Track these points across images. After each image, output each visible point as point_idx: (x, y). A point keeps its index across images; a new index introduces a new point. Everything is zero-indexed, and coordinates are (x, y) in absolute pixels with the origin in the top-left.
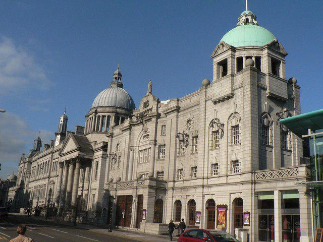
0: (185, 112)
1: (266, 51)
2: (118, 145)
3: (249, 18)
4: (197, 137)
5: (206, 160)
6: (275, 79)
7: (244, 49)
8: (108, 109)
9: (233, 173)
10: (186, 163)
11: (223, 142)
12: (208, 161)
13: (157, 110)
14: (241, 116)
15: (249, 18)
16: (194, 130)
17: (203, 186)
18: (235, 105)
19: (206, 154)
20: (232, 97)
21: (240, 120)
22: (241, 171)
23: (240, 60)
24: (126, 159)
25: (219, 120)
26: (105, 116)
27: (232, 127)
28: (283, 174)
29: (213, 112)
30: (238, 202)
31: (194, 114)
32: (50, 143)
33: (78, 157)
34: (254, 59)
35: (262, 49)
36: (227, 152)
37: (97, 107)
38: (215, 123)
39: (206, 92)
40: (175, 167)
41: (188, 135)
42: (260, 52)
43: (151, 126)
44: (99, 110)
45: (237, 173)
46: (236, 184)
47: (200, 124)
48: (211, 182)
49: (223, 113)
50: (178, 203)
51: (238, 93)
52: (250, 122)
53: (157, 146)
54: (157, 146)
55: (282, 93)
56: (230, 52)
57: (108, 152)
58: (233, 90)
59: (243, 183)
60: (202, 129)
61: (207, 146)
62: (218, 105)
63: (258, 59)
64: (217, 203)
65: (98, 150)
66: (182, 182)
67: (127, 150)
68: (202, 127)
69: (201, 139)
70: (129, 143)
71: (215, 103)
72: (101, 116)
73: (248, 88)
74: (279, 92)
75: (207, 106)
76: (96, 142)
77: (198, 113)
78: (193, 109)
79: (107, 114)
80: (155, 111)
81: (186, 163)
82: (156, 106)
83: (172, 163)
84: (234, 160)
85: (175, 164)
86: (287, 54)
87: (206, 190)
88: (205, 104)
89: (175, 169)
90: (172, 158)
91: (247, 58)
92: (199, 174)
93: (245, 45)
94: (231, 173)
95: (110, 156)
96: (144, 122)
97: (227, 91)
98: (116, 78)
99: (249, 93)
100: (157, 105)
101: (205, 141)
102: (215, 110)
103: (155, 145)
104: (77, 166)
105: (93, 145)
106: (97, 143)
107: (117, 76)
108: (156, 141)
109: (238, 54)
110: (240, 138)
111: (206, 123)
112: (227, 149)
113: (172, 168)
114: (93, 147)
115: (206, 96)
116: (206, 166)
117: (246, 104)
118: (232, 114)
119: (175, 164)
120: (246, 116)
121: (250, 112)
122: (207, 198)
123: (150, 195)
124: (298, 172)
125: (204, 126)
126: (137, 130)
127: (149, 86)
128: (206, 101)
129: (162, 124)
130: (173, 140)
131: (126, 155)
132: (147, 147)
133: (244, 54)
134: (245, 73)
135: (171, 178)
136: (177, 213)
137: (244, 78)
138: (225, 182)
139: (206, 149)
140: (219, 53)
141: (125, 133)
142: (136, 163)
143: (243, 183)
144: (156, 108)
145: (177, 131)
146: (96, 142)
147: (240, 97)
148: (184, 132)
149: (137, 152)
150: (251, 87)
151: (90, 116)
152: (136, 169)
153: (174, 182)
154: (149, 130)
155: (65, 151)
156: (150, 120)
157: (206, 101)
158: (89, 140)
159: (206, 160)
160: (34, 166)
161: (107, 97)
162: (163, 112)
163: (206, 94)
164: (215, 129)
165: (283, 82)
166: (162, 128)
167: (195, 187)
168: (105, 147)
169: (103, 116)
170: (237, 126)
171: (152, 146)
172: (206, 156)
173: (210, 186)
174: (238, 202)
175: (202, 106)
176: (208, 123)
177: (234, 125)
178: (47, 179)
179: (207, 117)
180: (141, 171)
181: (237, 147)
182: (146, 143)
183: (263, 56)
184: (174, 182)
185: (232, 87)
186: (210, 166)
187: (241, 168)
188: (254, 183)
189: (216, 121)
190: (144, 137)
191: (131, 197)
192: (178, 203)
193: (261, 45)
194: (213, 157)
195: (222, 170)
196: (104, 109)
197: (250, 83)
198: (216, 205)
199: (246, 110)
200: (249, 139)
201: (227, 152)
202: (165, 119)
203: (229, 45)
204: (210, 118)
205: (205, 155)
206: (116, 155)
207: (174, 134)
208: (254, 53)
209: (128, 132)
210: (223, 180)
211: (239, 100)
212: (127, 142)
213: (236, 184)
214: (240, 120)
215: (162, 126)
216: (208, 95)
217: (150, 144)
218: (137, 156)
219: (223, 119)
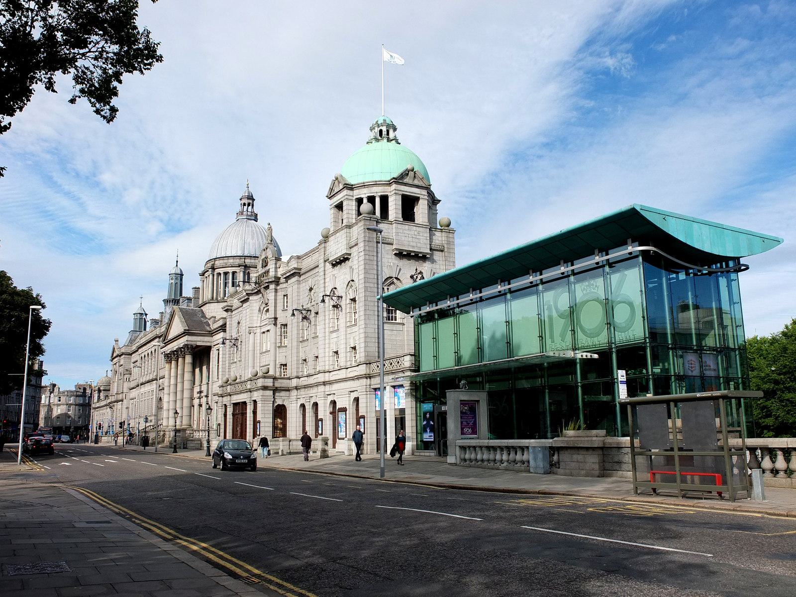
0: (307, 275)
2: (239, 323)
7: (364, 186)
13: (276, 271)
19: (381, 327)
20: (348, 259)
26: (228, 272)
41: (311, 311)
43: (270, 295)
44: (218, 263)
53: (279, 326)
54: (279, 326)
55: (419, 245)
59: (358, 378)
63: (384, 199)
72: (221, 272)
74: (414, 244)
79: (230, 270)
80: (274, 273)
82: (274, 266)
85: (298, 352)
96: (262, 290)
100: (276, 264)
103: (275, 324)
104: (189, 359)
105: (210, 322)
108: (276, 319)
109: (358, 193)
119: (298, 352)
129: (283, 293)
140: (336, 191)
141: (245, 305)
142: (258, 352)
143: (358, 378)
144: (273, 270)
146: (215, 317)
148: (303, 306)
149: (258, 334)
151: (206, 275)
155: (170, 337)
156: (267, 288)
160: (135, 360)
166: (284, 298)
169: (226, 274)
173: (330, 383)
178: (155, 382)
191: (245, 403)
196: (226, 261)
198: (337, 408)
202: (284, 285)
208: (377, 191)
211: (355, 262)
215: (284, 296)
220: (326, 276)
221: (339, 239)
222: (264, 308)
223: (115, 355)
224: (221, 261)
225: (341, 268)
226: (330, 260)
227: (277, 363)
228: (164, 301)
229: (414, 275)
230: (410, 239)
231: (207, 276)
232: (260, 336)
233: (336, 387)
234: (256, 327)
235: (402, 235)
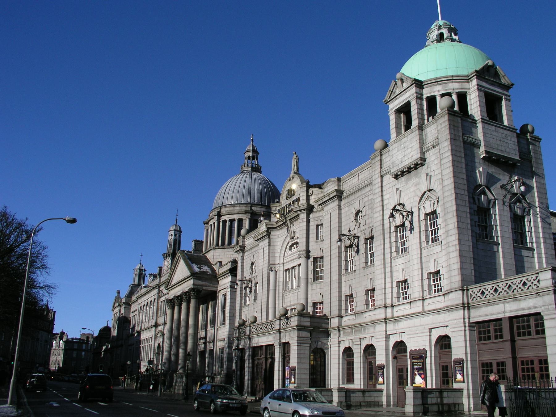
1: (475, 82)
2: (253, 264)
3: (445, 32)
4: (372, 238)
5: (388, 275)
6: (493, 128)
7: (437, 81)
8: (237, 208)
9: (433, 294)
10: (356, 285)
11: (413, 240)
12: (392, 277)
14: (439, 194)
15: (445, 32)
16: (366, 227)
18: (429, 177)
21: (438, 202)
22: (445, 289)
23: (432, 101)
24: (265, 286)
25: (404, 205)
26: (234, 220)
27: (427, 215)
28: (514, 287)
30: (444, 342)
31: (366, 199)
32: (156, 272)
33: (192, 289)
34: (454, 97)
35: (467, 79)
36: (421, 258)
37: (221, 207)
38: (398, 210)
39: (381, 160)
40: (340, 292)
41: (358, 237)
42: (466, 85)
43: (299, 227)
44: (223, 211)
45: (440, 293)
46: (437, 311)
47: (376, 215)
48: (399, 311)
49: (409, 192)
50: (348, 352)
51: (431, 156)
52: (454, 202)
53: (311, 260)
54: (311, 260)
55: (508, 150)
57: (239, 277)
58: (423, 153)
59: (449, 309)
60: (378, 224)
62: (403, 179)
63: (462, 97)
64: (411, 346)
65: (224, 275)
66: (353, 317)
67: (266, 272)
68: (376, 220)
69: (377, 242)
70: (269, 259)
71: (396, 177)
72: (227, 220)
73: (446, 146)
74: (503, 149)
75: (384, 184)
76: (221, 263)
77: (370, 197)
78: (363, 192)
79: (236, 217)
80: (305, 201)
81: (356, 285)
82: (305, 194)
83: (335, 285)
84: (433, 270)
85: (340, 287)
86: (513, 85)
87: (391, 328)
88: (382, 182)
89: (340, 296)
90: (335, 277)
91: (443, 95)
92: (379, 298)
93: (439, 75)
94: (430, 293)
95: (242, 284)
96: (288, 222)
97: (413, 155)
98: (249, 157)
99: (449, 153)
100: (307, 192)
102: (397, 189)
103: (308, 257)
106: (223, 264)
107: (250, 154)
108: (308, 251)
109: (427, 92)
110: (440, 233)
111: (385, 212)
112: (421, 254)
113: (335, 294)
114: (217, 271)
115: (381, 168)
116: (388, 285)
117: (445, 172)
118: (425, 192)
119: (340, 287)
120: (446, 194)
121: (452, 186)
122: (393, 340)
123: (300, 342)
124: (539, 281)
125: (381, 218)
126: (280, 237)
127: (294, 161)
128: (382, 177)
129: (316, 223)
130: (336, 245)
131: (265, 279)
132: (295, 263)
133: (437, 91)
134: (441, 121)
135: (336, 312)
136: (348, 369)
137: (439, 129)
138: (421, 309)
139: (388, 256)
140: (397, 93)
142: (281, 291)
143: (449, 309)
145: (340, 230)
146: (221, 263)
147: (436, 162)
148: (350, 231)
149: (281, 272)
150: (451, 144)
151: (211, 223)
152: (281, 301)
153: (340, 316)
154: (297, 235)
155: (174, 282)
157: (382, 177)
158: (211, 261)
159: (388, 275)
160: (134, 309)
161: (234, 190)
162: (317, 202)
163: (381, 164)
164: (399, 220)
165: (508, 133)
167: (374, 323)
168: (233, 271)
169: (232, 221)
170: (434, 213)
171: (302, 261)
172: (388, 270)
173: (396, 320)
174: (444, 342)
175: (377, 186)
176: (387, 213)
177: (429, 211)
178: (154, 329)
179: (385, 203)
180: (289, 304)
181: (437, 248)
182: (294, 258)
183: (472, 90)
184: (340, 316)
185: (421, 148)
186: (395, 284)
187: (445, 283)
188: (466, 306)
189: (398, 207)
190: (291, 246)
192: (348, 352)
193: (466, 73)
195: (415, 291)
196: (232, 208)
197: (448, 137)
198: (409, 351)
199: (446, 183)
200: (455, 231)
201: (421, 258)
202: (321, 213)
203: (411, 78)
204: (391, 202)
205: (384, 270)
206: (250, 281)
207: (335, 237)
208: (455, 87)
209: (267, 241)
210: (417, 307)
211: (434, 167)
212: (266, 258)
213: (437, 311)
214: (438, 202)
215: (318, 226)
216: (384, 166)
217: (299, 257)
218: (281, 280)
219: (411, 203)
220: (384, 193)
221: (406, 145)
223: (116, 305)
224: (227, 209)
225: (407, 182)
227: (309, 301)
228: (163, 255)
229: (507, 184)
230: (498, 142)
231: (212, 223)
233: (402, 325)
235: (489, 136)
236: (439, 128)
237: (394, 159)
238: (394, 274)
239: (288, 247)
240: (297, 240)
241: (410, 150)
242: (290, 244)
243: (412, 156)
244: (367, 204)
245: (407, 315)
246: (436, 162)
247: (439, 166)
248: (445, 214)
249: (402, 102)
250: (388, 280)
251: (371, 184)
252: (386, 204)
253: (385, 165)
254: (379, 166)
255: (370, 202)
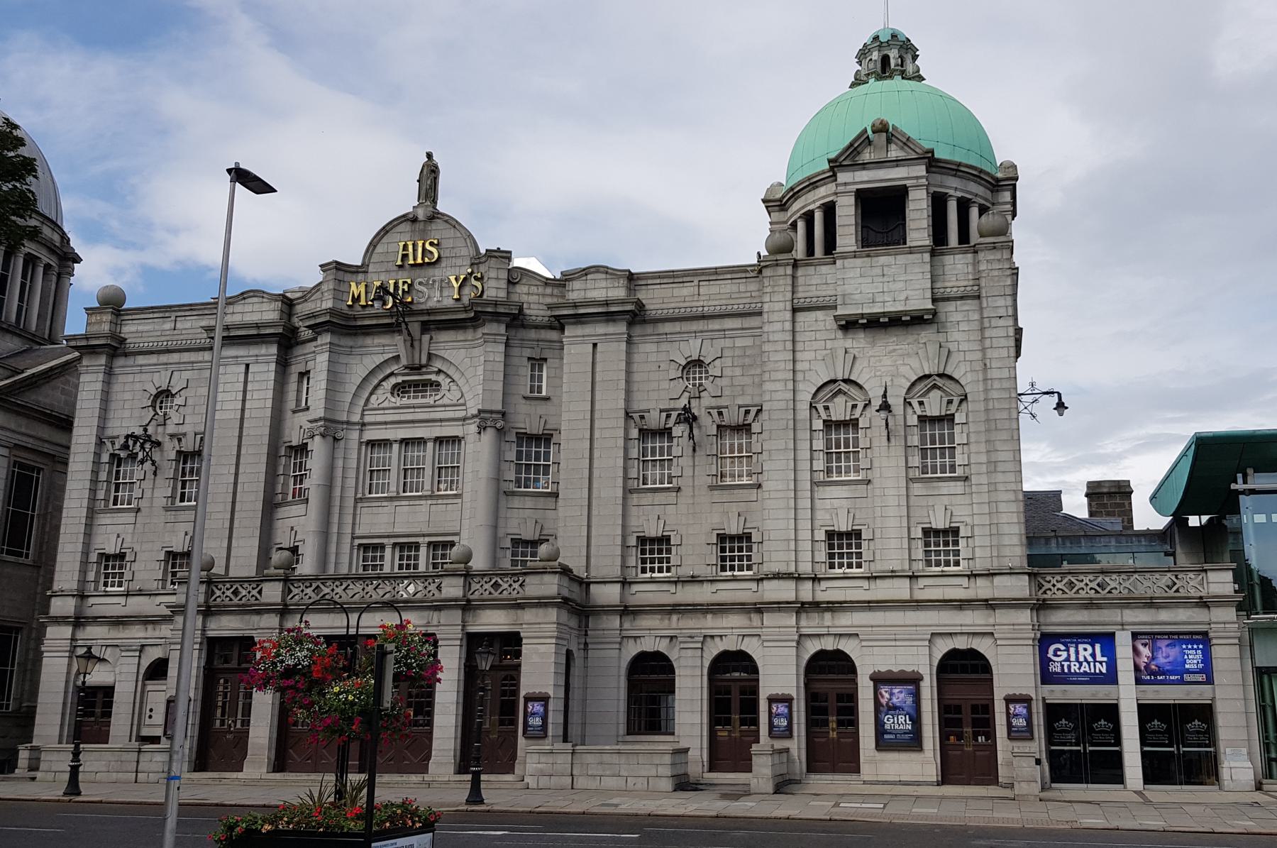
0: (668, 328)
17: (803, 608)
29: (823, 351)
30: (964, 667)
31: (728, 343)
39: (794, 277)
48: (827, 592)
56: (921, 170)
61: (804, 465)
71: (849, 325)
78: (715, 324)
87: (810, 623)
88: (794, 322)
97: (920, 301)
101: (781, 457)
116: (805, 535)
129: (528, 353)
139: (805, 476)
142: (350, 493)
149: (354, 445)
152: (349, 519)
157: (795, 310)
173: (834, 607)
188: (1041, 606)
194: (837, 508)
222: (392, 374)
226: (839, 312)
227: (501, 533)
232: (360, 450)
233: (846, 620)
234: (348, 423)
236: (983, 267)
237: (848, 289)
238: (819, 515)
239: (388, 385)
240: (433, 377)
241: (901, 285)
242: (393, 381)
243: (907, 299)
244: (726, 353)
245: (869, 602)
246: (963, 326)
247: (977, 336)
248: (988, 431)
249: (882, 181)
250: (805, 525)
251: (760, 314)
252: (804, 372)
253: (800, 289)
254: (790, 288)
255: (738, 352)
